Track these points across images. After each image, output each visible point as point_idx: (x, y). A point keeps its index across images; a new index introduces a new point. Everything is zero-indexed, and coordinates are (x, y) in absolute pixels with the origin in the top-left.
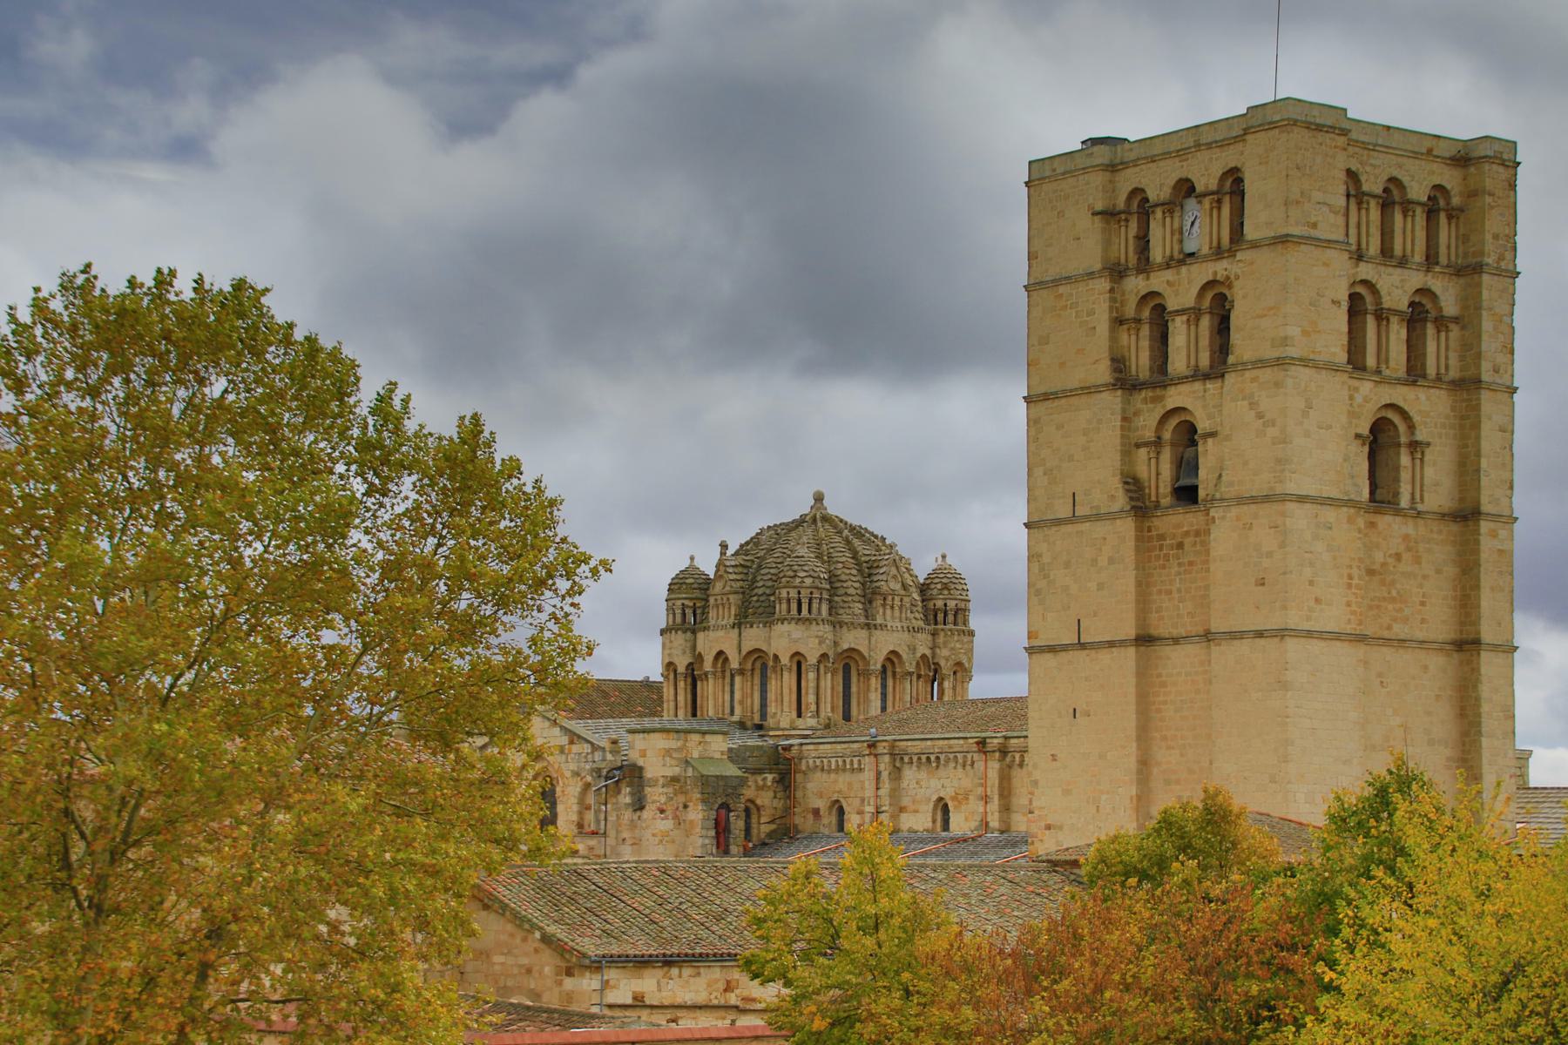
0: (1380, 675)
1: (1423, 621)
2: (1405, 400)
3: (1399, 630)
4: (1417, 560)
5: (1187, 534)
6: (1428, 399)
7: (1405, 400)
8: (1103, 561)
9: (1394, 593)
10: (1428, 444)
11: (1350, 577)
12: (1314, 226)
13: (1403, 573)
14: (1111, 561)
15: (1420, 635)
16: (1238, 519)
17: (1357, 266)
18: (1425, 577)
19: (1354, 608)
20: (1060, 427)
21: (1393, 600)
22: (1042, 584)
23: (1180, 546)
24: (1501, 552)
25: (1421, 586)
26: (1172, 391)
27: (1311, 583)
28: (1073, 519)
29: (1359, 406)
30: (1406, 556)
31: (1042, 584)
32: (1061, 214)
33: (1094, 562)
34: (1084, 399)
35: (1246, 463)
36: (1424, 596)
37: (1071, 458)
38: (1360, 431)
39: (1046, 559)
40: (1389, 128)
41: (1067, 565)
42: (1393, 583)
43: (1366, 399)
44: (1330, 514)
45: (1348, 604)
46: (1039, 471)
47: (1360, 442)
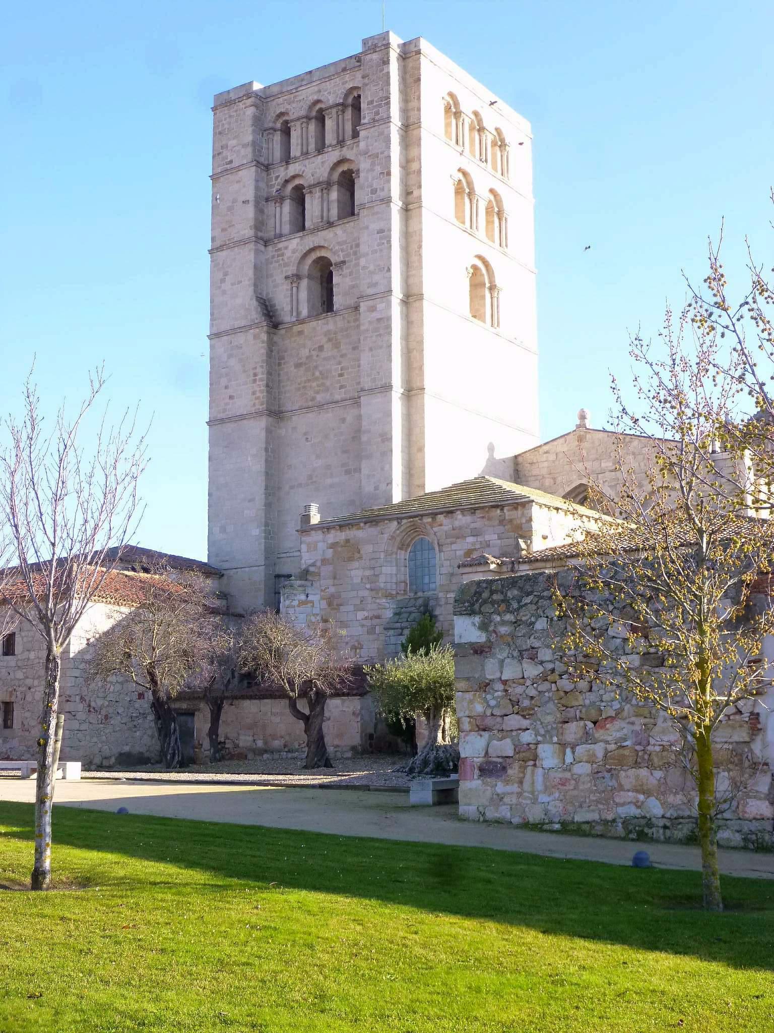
0: (305, 434)
1: (341, 387)
2: (325, 240)
3: (319, 398)
4: (337, 345)
6: (344, 231)
7: (325, 240)
9: (317, 374)
10: (344, 262)
11: (255, 375)
12: (231, 162)
13: (325, 359)
15: (337, 397)
17: (287, 169)
18: (342, 356)
19: (258, 394)
21: (317, 379)
24: (379, 320)
25: (339, 363)
27: (226, 387)
29: (289, 258)
30: (325, 346)
36: (341, 370)
38: (289, 273)
40: (311, 72)
42: (316, 367)
43: (294, 251)
44: (240, 339)
45: (254, 393)
47: (289, 281)
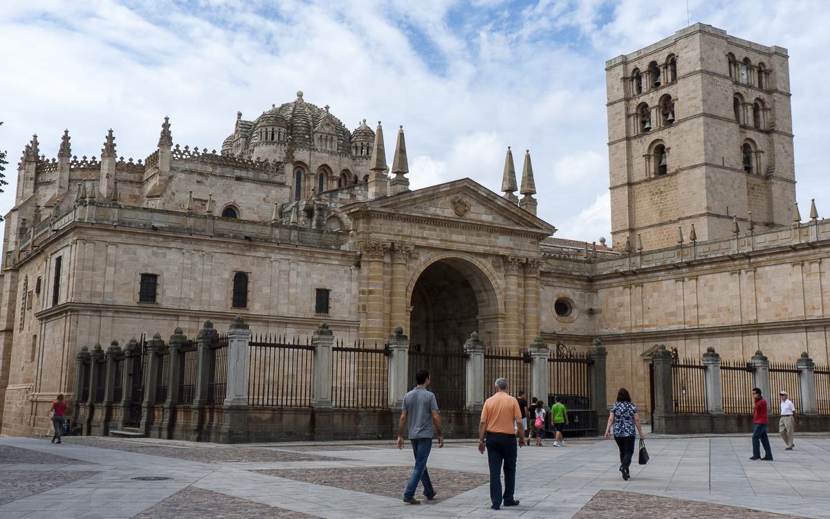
5: (755, 185)
8: (735, 186)
14: (738, 187)
16: (781, 185)
20: (716, 129)
22: (711, 189)
23: (753, 189)
26: (748, 131)
28: (723, 167)
31: (711, 189)
32: (712, 49)
33: (732, 186)
34: (726, 123)
35: (783, 167)
37: (721, 143)
39: (713, 179)
41: (722, 184)
46: (709, 144)
